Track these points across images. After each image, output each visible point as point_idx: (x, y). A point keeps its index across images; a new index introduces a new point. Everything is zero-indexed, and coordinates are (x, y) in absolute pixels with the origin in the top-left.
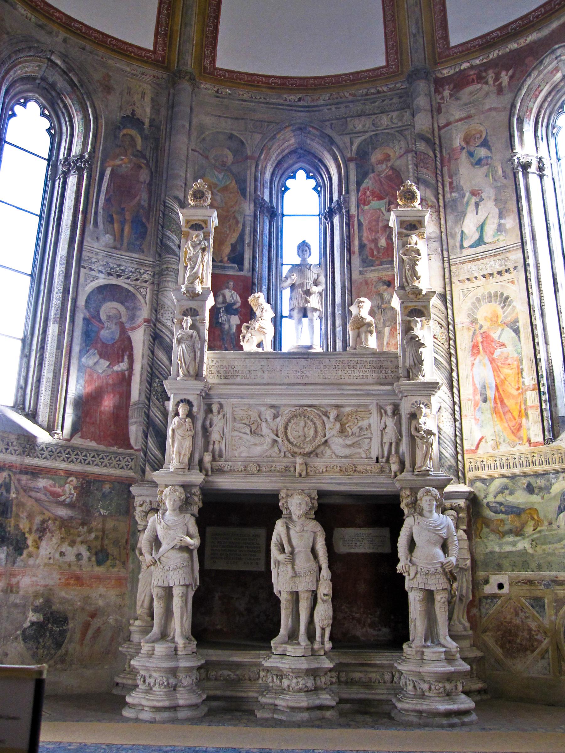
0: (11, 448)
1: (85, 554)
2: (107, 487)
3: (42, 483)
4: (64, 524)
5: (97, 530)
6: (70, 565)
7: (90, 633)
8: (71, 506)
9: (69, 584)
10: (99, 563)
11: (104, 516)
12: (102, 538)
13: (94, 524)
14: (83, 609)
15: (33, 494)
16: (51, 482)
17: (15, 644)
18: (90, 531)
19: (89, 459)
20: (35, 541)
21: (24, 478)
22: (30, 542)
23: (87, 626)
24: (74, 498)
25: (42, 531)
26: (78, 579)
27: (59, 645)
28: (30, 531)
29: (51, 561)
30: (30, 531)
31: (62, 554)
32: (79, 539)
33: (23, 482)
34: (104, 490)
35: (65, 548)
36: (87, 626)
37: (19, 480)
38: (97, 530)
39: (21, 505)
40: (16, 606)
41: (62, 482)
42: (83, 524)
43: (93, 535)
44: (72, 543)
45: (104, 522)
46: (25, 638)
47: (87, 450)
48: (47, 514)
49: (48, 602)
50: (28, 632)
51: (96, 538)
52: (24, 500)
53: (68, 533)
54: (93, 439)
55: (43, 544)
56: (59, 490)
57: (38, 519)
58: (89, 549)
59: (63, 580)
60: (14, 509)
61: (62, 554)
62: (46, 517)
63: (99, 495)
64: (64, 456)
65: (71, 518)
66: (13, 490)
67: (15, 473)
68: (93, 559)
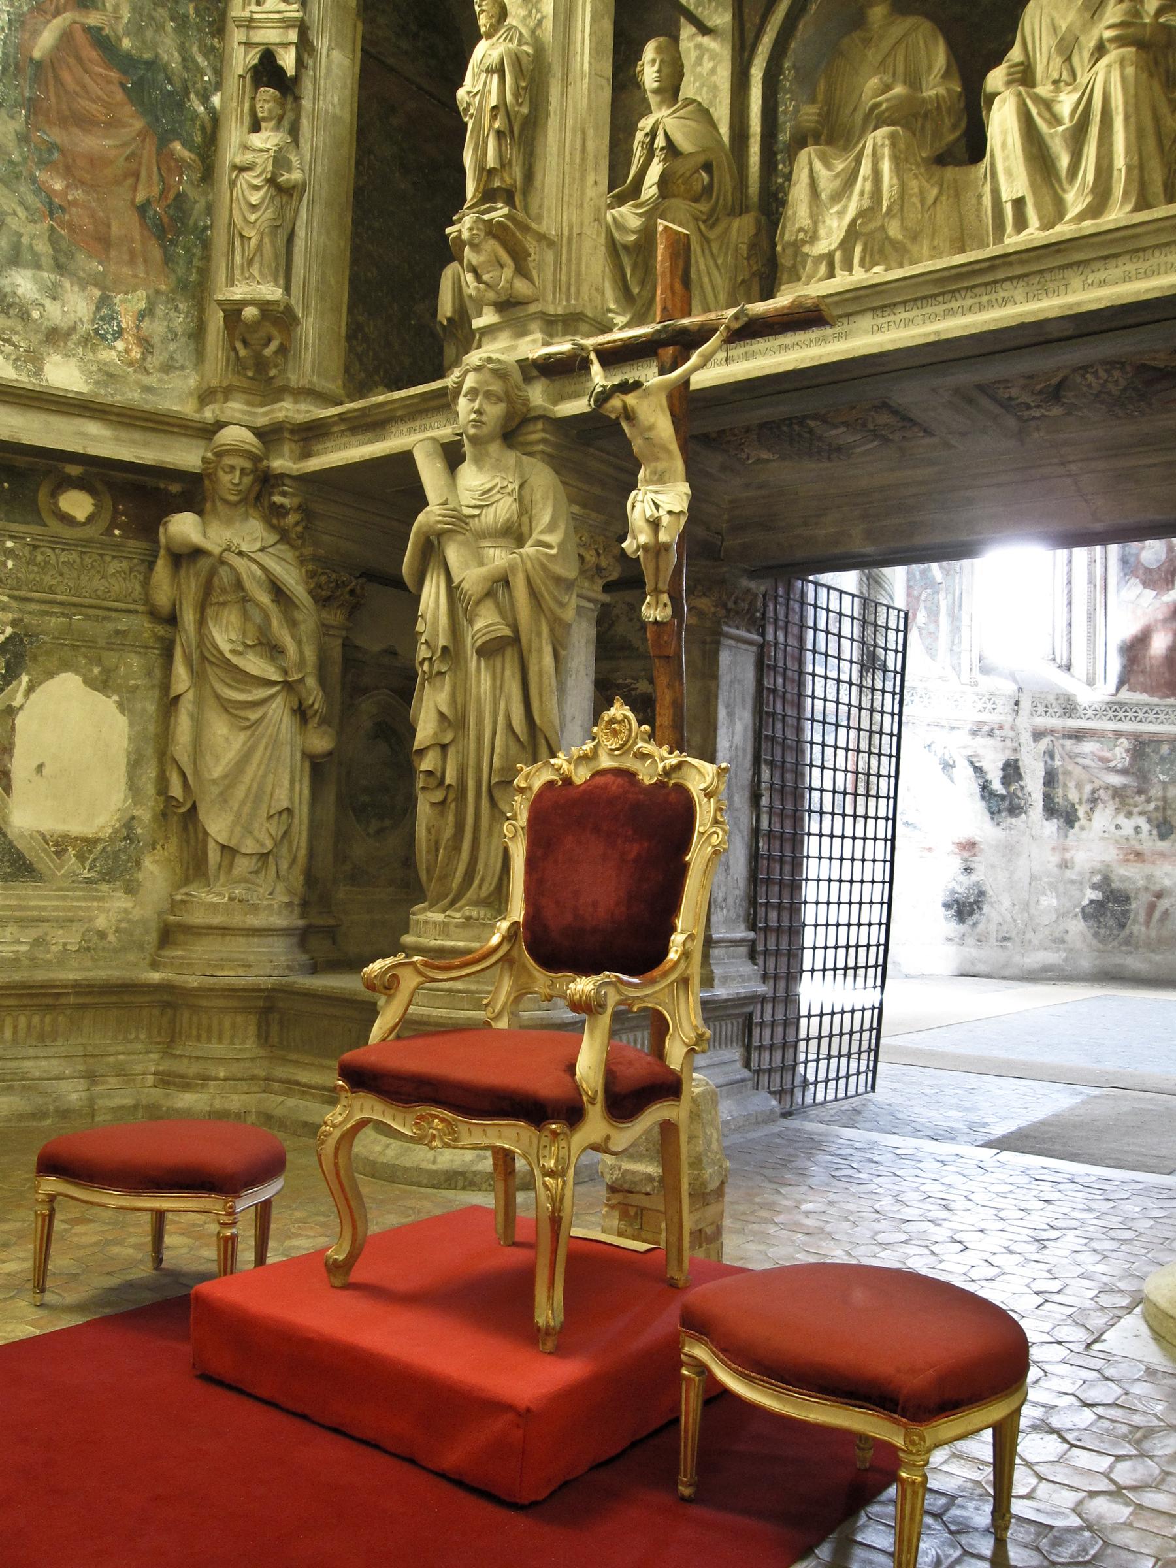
0: (1050, 710)
1: (1145, 827)
2: (1165, 749)
3: (1089, 747)
4: (1118, 793)
5: (1157, 799)
6: (1127, 839)
7: (1157, 915)
8: (1124, 772)
9: (1128, 860)
10: (1162, 837)
11: (1164, 782)
12: (1164, 809)
13: (1152, 792)
14: (1147, 889)
15: (1080, 760)
16: (1098, 745)
17: (1075, 922)
18: (1148, 801)
19: (1141, 715)
20: (1086, 812)
21: (1068, 743)
22: (1081, 813)
23: (1152, 908)
24: (1127, 763)
25: (1094, 801)
26: (1138, 855)
27: (1122, 926)
28: (1080, 802)
29: (1106, 835)
30: (1080, 802)
31: (1118, 827)
32: (1136, 810)
33: (1068, 748)
34: (1162, 751)
35: (1121, 819)
36: (1152, 908)
37: (1063, 746)
38: (1157, 799)
39: (1067, 773)
40: (1073, 882)
41: (1111, 744)
42: (1140, 792)
43: (1152, 806)
44: (1129, 815)
45: (1165, 789)
46: (1085, 916)
47: (1137, 704)
48: (1097, 783)
49: (1106, 880)
50: (1087, 910)
51: (1157, 809)
52: (1070, 767)
53: (1123, 803)
54: (1144, 690)
55: (1096, 816)
56: (1108, 755)
57: (1088, 788)
58: (1149, 821)
59: (1121, 856)
60: (1061, 777)
61: (1118, 827)
62: (1096, 785)
63: (1156, 758)
64: (1111, 714)
65: (1125, 786)
66: (1057, 757)
67: (1057, 738)
68: (1155, 832)
